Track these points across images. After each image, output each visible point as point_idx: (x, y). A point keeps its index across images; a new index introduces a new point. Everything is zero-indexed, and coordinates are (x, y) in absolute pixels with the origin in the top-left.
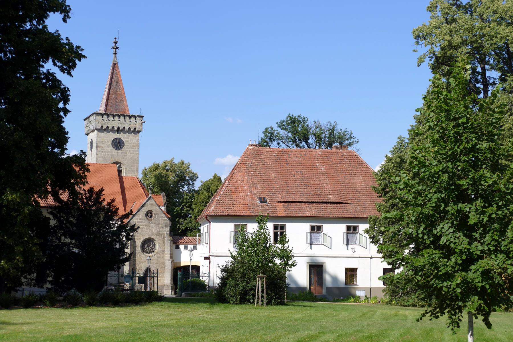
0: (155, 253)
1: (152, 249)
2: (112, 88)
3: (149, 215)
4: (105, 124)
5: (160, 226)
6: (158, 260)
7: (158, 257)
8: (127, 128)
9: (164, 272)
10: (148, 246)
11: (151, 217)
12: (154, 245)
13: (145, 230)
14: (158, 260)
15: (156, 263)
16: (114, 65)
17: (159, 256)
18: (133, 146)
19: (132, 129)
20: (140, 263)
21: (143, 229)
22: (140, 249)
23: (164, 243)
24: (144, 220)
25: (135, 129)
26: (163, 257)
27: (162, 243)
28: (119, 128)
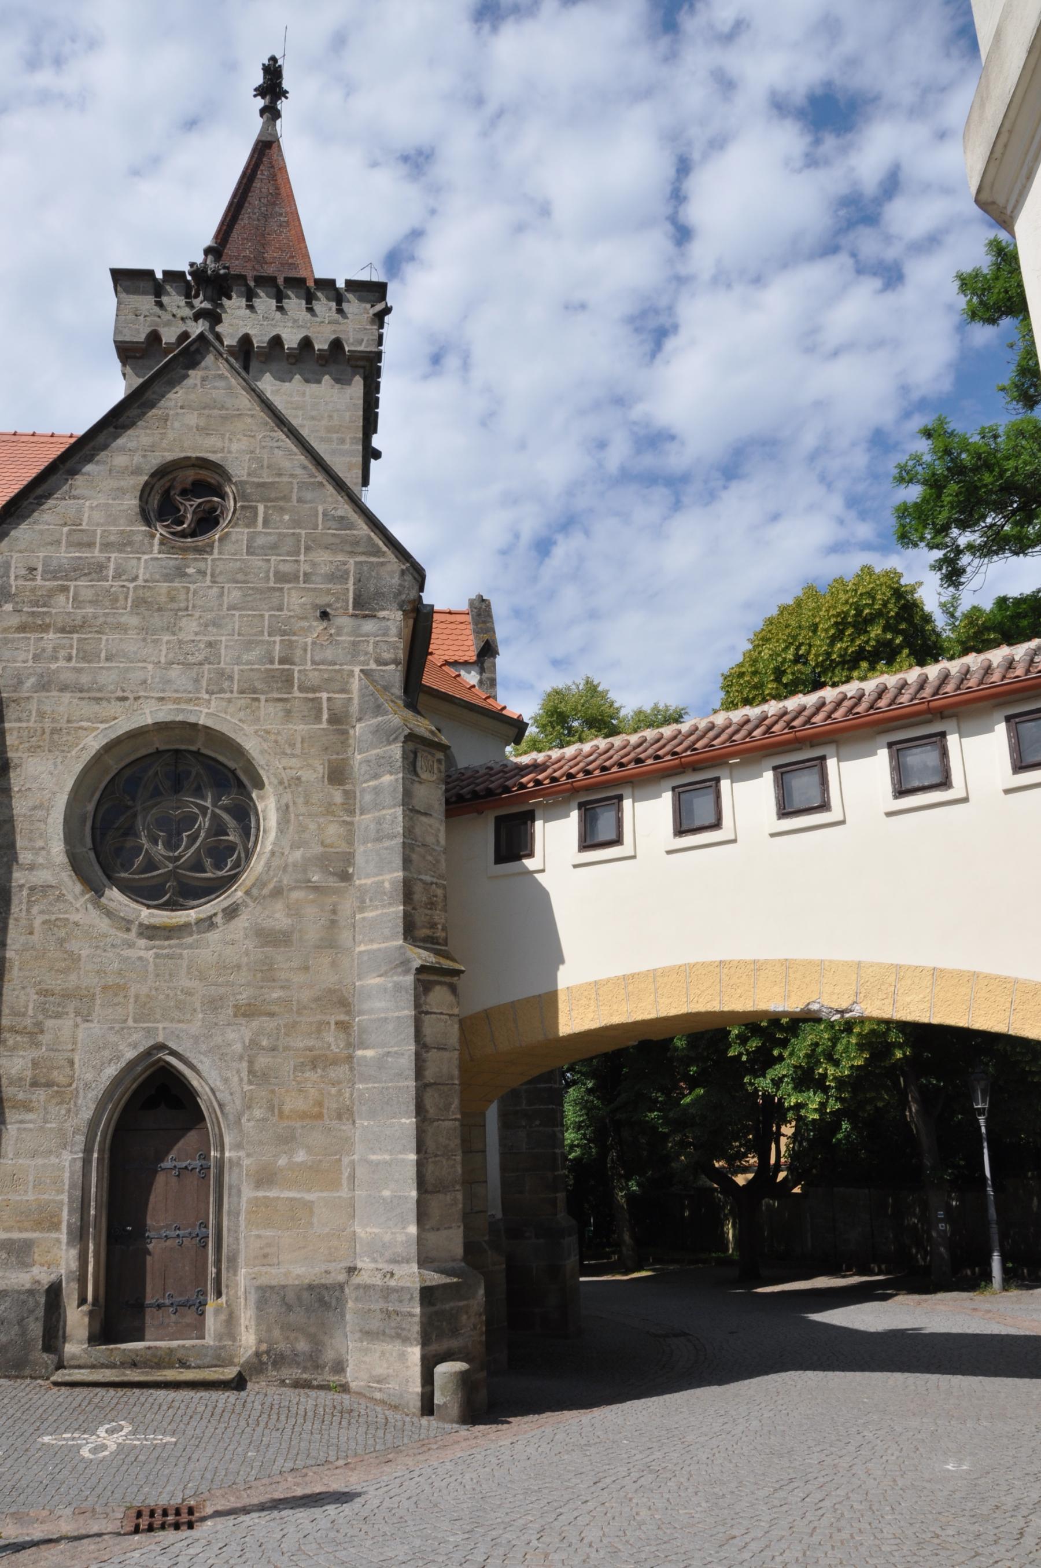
0: (237, 893)
1: (220, 853)
2: (244, 220)
3: (189, 508)
4: (168, 324)
5: (296, 600)
6: (267, 972)
7: (272, 939)
8: (291, 340)
9: (346, 1114)
10: (173, 831)
11: (207, 521)
12: (244, 815)
13: (131, 644)
14: (267, 972)
15: (248, 1012)
16: (265, 152)
17: (278, 917)
18: (329, 430)
19: (321, 345)
20: (55, 1001)
21: (108, 641)
22: (57, 848)
23: (338, 775)
24: (124, 544)
25: (337, 345)
26: (329, 943)
27: (314, 773)
28: (246, 340)
